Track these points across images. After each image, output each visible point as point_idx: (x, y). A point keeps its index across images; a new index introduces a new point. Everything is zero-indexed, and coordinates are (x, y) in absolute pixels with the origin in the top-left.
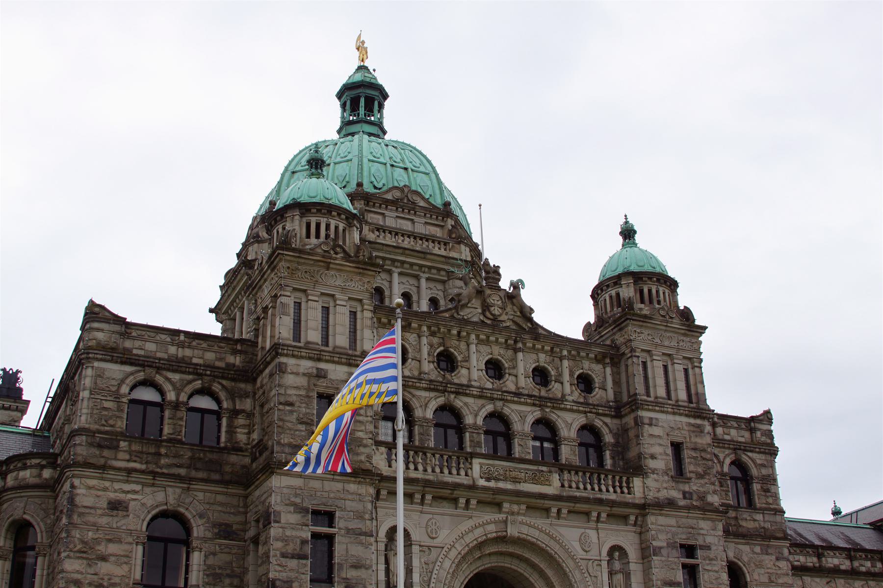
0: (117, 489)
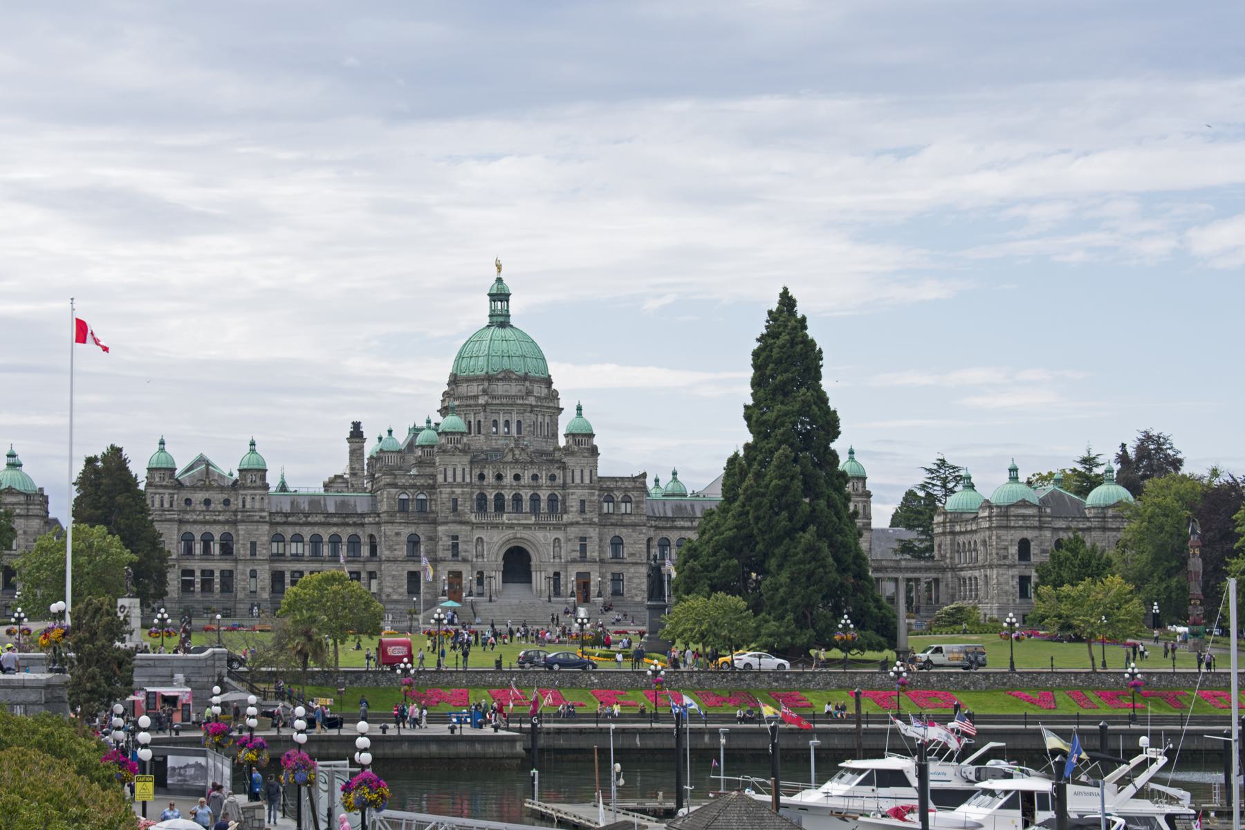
0: (397, 528)
